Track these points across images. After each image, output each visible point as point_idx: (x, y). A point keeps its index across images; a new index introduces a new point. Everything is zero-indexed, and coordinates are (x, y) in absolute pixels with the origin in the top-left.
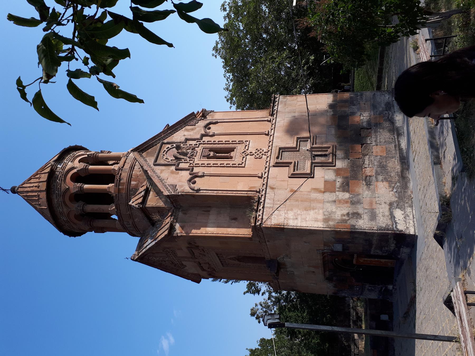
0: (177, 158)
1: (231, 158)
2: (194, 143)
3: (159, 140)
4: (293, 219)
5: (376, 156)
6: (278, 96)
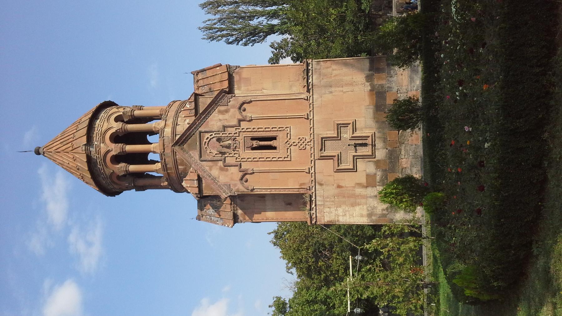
0: (221, 153)
1: (275, 148)
2: (232, 130)
3: (195, 128)
4: (343, 216)
5: (412, 145)
6: (310, 60)
